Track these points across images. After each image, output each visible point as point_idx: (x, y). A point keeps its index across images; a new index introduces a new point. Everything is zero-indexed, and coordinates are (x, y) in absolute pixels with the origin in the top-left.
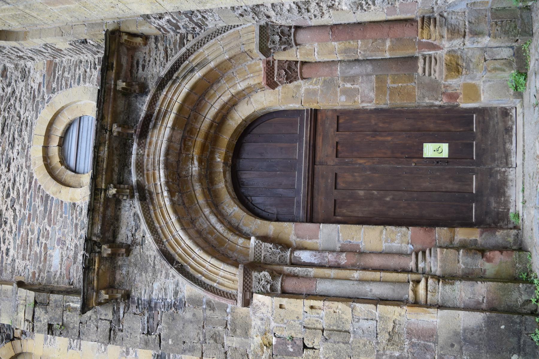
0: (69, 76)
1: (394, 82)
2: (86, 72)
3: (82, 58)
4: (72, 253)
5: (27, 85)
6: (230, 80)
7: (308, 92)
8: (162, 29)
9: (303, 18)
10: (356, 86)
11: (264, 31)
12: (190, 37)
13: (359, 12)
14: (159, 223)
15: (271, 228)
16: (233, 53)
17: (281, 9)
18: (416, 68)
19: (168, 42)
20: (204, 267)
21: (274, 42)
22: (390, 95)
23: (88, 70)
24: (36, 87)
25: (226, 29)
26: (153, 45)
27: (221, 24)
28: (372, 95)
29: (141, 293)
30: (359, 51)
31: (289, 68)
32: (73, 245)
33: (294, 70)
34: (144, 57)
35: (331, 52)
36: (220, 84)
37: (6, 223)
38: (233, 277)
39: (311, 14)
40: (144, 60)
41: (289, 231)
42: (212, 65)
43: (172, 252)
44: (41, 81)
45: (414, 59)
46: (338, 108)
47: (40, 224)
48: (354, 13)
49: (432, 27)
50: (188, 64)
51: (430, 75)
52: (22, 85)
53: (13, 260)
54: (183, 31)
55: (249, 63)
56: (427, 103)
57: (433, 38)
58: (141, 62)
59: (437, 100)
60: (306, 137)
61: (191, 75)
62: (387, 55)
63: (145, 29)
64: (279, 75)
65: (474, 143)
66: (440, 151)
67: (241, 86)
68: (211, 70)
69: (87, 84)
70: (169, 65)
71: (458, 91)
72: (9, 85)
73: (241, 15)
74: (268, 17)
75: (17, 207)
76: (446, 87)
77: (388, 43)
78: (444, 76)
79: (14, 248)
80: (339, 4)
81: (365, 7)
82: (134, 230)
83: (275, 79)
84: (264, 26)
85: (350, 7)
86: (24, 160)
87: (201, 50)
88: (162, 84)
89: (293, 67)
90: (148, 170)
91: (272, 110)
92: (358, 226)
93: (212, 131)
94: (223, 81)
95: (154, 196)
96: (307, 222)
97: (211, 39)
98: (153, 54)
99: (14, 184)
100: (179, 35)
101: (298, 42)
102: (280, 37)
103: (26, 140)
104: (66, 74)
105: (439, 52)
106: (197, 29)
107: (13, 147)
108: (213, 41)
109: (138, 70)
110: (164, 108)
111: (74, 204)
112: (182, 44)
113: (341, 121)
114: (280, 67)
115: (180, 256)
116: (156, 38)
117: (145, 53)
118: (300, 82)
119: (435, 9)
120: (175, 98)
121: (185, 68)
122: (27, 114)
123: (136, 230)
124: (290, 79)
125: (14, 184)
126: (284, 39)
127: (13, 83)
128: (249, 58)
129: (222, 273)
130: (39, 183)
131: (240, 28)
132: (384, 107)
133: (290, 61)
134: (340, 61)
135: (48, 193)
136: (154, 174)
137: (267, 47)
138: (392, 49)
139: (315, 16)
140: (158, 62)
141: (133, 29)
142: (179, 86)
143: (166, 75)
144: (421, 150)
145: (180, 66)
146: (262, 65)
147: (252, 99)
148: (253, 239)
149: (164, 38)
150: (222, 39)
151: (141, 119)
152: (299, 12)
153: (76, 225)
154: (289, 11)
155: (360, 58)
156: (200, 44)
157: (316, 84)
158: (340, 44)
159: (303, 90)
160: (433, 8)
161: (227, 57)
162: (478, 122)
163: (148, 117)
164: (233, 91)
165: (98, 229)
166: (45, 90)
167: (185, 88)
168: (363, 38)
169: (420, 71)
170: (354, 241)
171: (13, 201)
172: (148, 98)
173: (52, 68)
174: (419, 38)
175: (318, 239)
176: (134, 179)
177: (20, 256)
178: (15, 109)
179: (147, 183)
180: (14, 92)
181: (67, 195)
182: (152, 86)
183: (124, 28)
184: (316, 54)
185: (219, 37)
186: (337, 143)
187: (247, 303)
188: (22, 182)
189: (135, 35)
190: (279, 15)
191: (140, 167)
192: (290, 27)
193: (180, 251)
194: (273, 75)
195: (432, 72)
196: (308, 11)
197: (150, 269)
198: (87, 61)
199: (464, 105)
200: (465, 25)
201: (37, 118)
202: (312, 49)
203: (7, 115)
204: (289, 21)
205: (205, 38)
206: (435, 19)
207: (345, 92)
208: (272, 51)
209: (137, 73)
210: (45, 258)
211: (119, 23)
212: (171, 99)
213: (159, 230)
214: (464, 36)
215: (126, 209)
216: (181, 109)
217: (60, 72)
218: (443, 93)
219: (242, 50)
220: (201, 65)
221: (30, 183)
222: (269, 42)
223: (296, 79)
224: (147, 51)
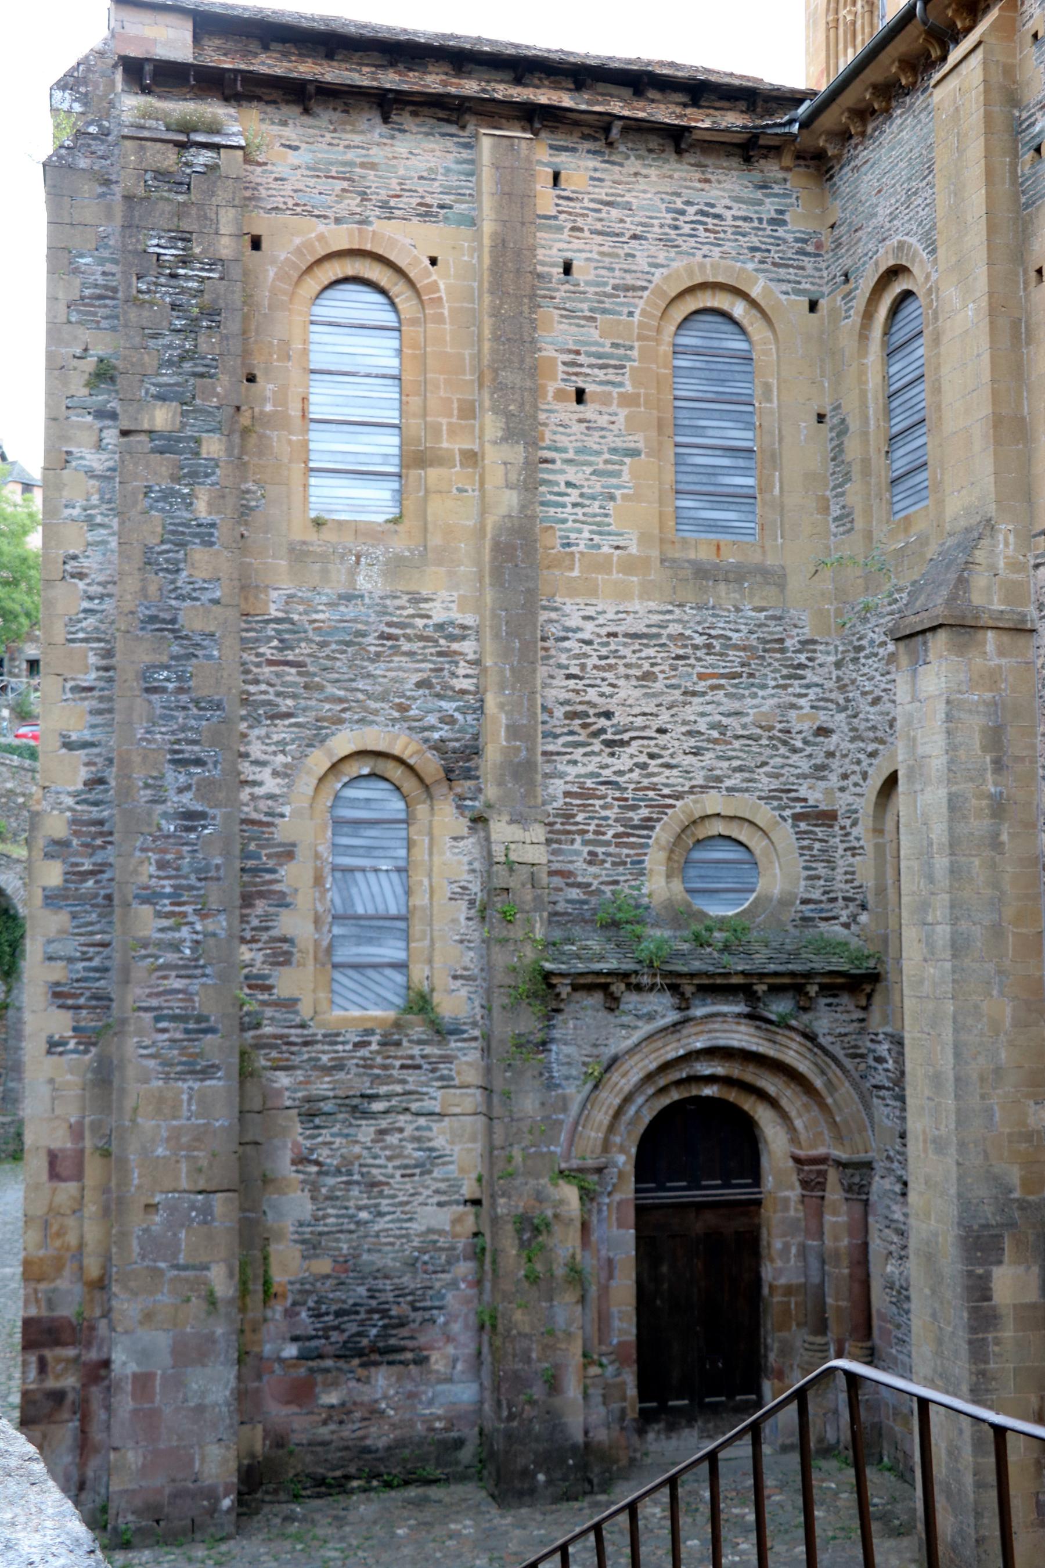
4: (580, 879)
5: (805, 776)
7: (787, 1200)
24: (803, 792)
37: (612, 755)
44: (811, 803)
47: (616, 820)
52: (805, 766)
53: (561, 775)
67: (798, 1123)
69: (803, 883)
72: (806, 742)
75: (635, 775)
79: (578, 776)
86: (701, 782)
88: (810, 1037)
91: (761, 1146)
94: (805, 1099)
95: (677, 1036)
98: (845, 1017)
99: (668, 766)
103: (728, 783)
104: (817, 845)
107: (719, 758)
110: (779, 1038)
116: (862, 1020)
122: (765, 780)
124: (805, 1184)
125: (668, 766)
127: (809, 750)
130: (669, 811)
135: (658, 826)
141: (877, 999)
149: (862, 1031)
153: (616, 882)
159: (787, 1193)
164: (793, 1114)
166: (798, 810)
169: (811, 1339)
171: (644, 766)
173: (828, 817)
177: (569, 788)
178: (772, 757)
180: (795, 750)
181: (655, 860)
188: (671, 781)
189: (869, 996)
201: (760, 798)
203: (764, 742)
207: (787, 1247)
210: (569, 832)
217: (820, 836)
221: (669, 796)
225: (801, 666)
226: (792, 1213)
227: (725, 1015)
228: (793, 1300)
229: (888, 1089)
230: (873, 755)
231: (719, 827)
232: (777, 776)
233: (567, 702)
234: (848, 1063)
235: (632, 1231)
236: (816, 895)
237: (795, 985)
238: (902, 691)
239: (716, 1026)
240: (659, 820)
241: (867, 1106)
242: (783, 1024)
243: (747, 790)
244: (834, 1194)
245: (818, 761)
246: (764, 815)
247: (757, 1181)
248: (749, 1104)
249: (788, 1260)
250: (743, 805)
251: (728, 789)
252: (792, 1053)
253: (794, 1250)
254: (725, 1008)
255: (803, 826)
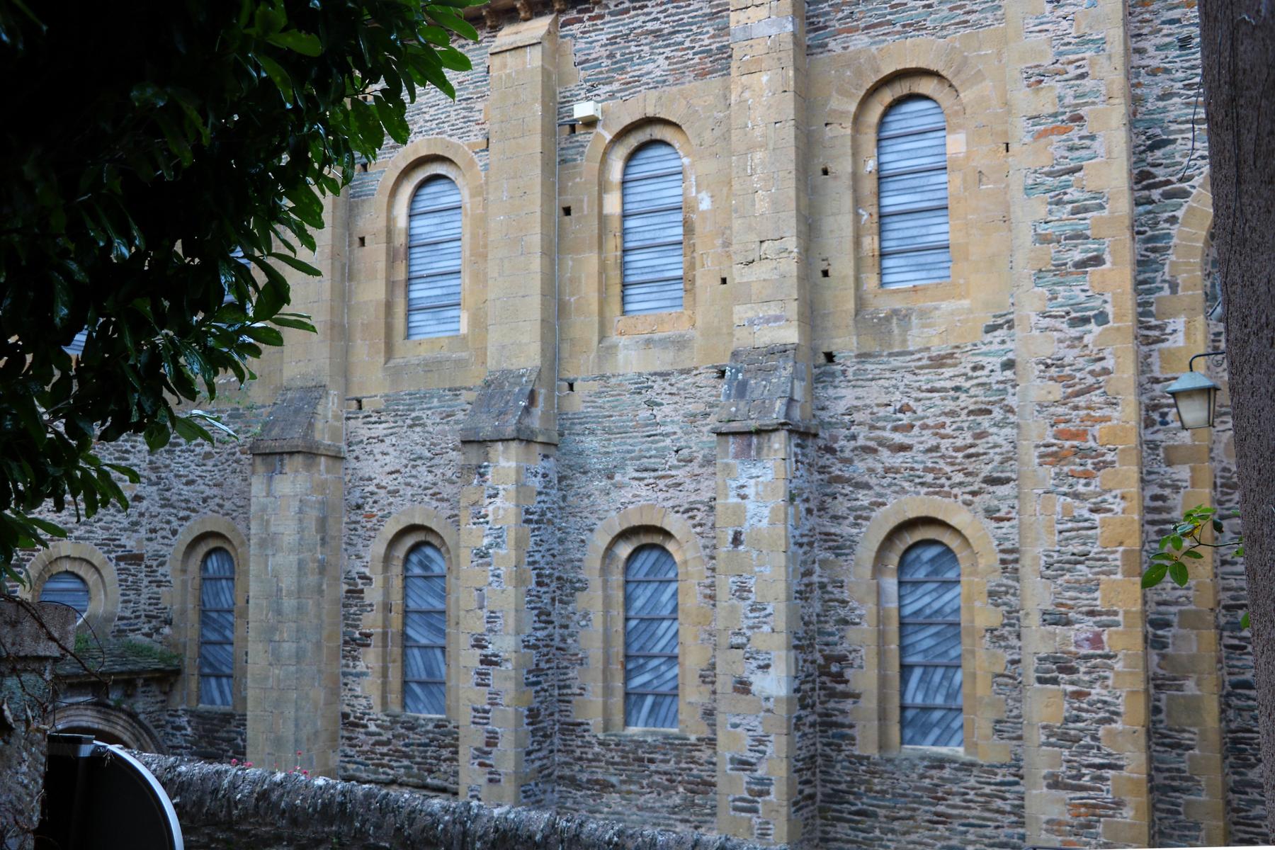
5: (125, 530)
24: (123, 542)
52: (125, 523)
88: (133, 716)
103: (76, 533)
104: (130, 579)
112: (156, 727)
122: (100, 532)
173: (137, 559)
189: (172, 685)
225: (127, 452)
227: (79, 704)
229: (186, 748)
230: (186, 518)
231: (67, 566)
232: (108, 529)
233: (766, 616)
234: (155, 732)
236: (128, 614)
237: (128, 683)
238: (257, 487)
239: (72, 712)
240: (28, 560)
242: (117, 708)
243: (88, 539)
245: (134, 519)
246: (98, 557)
250: (85, 549)
251: (76, 538)
254: (81, 699)
255: (122, 565)
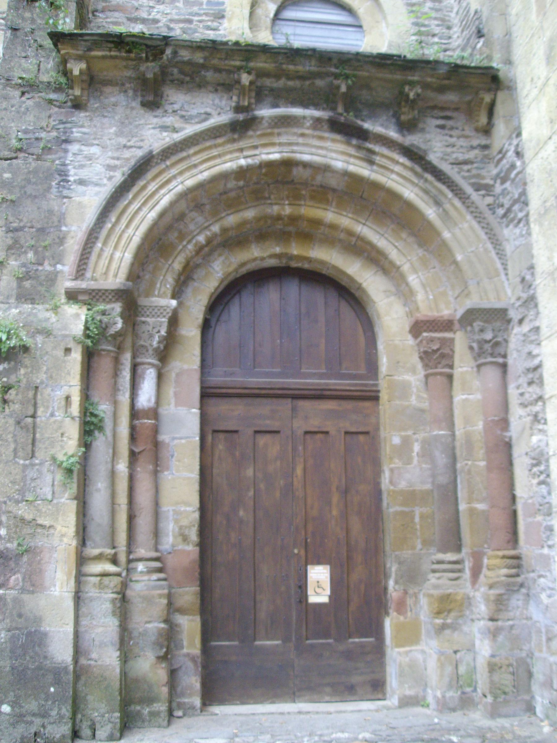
0: (426, 9)
1: (422, 517)
2: (434, 35)
3: (455, 29)
4: (145, 15)
6: (424, 262)
8: (500, 156)
9: (519, 376)
10: (415, 460)
11: (498, 317)
12: (489, 200)
13: (527, 461)
14: (195, 154)
15: (191, 332)
16: (465, 267)
17: (532, 342)
18: (444, 549)
19: (481, 165)
20: (127, 226)
21: (482, 331)
22: (403, 513)
23: (436, 40)
25: (501, 254)
26: (475, 142)
27: (509, 248)
28: (403, 485)
29: (82, 126)
30: (470, 463)
31: (443, 356)
32: (158, 17)
33: (439, 363)
34: (457, 129)
35: (467, 421)
36: (416, 246)
38: (111, 273)
39: (525, 388)
40: (452, 128)
41: (188, 360)
42: (446, 235)
43: (149, 175)
45: (458, 548)
46: (383, 433)
48: (527, 454)
49: (505, 571)
50: (446, 196)
51: (434, 571)
54: (498, 188)
55: (450, 293)
56: (390, 568)
57: (489, 573)
58: (450, 123)
59: (396, 582)
60: (335, 384)
61: (431, 201)
62: (462, 507)
63: (500, 128)
64: (432, 340)
65: (331, 641)
66: (318, 590)
67: (413, 280)
68: (439, 234)
70: (445, 167)
71: (409, 614)
73: (523, 280)
74: (521, 321)
76: (416, 595)
77: (481, 506)
78: (432, 592)
80: (540, 430)
81: (535, 469)
82: (183, 113)
83: (425, 334)
84: (506, 315)
85: (536, 446)
87: (469, 217)
89: (444, 362)
90: (279, 134)
91: (376, 329)
92: (198, 467)
93: (342, 236)
94: (420, 252)
96: (202, 388)
97: (486, 233)
98: (462, 142)
100: (491, 182)
101: (483, 369)
102: (490, 341)
105: (468, 584)
106: (501, 211)
108: (484, 236)
109: (437, 118)
111: (223, 17)
112: (478, 187)
113: (361, 438)
114: (443, 341)
115: (144, 188)
116: (486, 147)
117: (463, 130)
118: (421, 372)
119: (532, 575)
120: (394, 176)
121: (440, 192)
123: (182, 117)
126: (487, 346)
128: (457, 293)
129: (118, 255)
131: (503, 277)
132: (385, 504)
133: (452, 357)
134: (453, 435)
136: (273, 144)
137: (474, 320)
138: (472, 512)
139: (522, 394)
140: (449, 150)
141: (499, 109)
142: (412, 183)
143: (430, 163)
144: (319, 562)
145: (444, 183)
146: (446, 312)
147: (392, 298)
148: (174, 303)
149: (487, 159)
150: (486, 250)
151: (359, 122)
152: (528, 370)
154: (530, 353)
155: (459, 465)
156: (478, 216)
157: (419, 397)
158: (480, 433)
160: (533, 571)
161: (459, 258)
162: (362, 646)
163: (363, 135)
164: (406, 268)
165: (185, 55)
167: (409, 193)
168: (489, 468)
169: (440, 556)
170: (174, 463)
172: (393, 134)
174: (490, 553)
175: (176, 406)
176: (265, 112)
179: (259, 133)
182: (412, 140)
183: (501, 96)
184: (464, 397)
185: (489, 246)
186: (327, 433)
187: (72, 296)
190: (522, 338)
191: (285, 122)
192: (505, 356)
193: (152, 187)
194: (431, 331)
195: (437, 575)
196: (530, 383)
197: (123, 141)
198: (450, 38)
199: (388, 624)
200: (509, 620)
202: (471, 391)
204: (515, 355)
205: (488, 224)
206: (518, 575)
207: (406, 442)
208: (469, 328)
209: (433, 117)
211: (509, 88)
212: (392, 171)
213: (184, 154)
214: (492, 619)
215: (217, 101)
216: (376, 186)
218: (406, 592)
219: (470, 282)
220: (445, 216)
222: (482, 324)
223: (426, 366)
224: (467, 132)
226: (413, 401)
228: (418, 511)
235: (196, 411)
241: (496, 242)
244: (463, 365)
247: (377, 379)
248: (354, 269)
249: (409, 461)
252: (397, 178)
253: (416, 448)
